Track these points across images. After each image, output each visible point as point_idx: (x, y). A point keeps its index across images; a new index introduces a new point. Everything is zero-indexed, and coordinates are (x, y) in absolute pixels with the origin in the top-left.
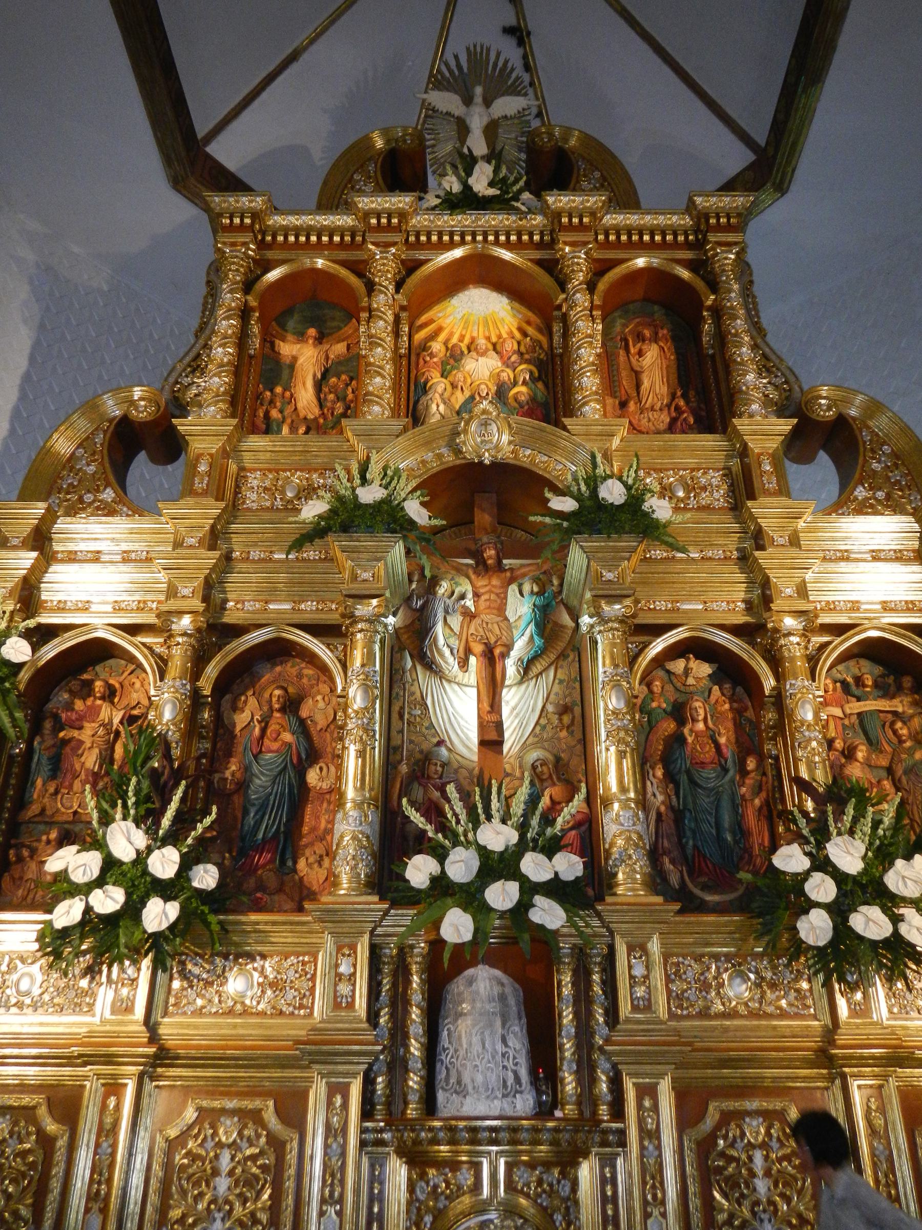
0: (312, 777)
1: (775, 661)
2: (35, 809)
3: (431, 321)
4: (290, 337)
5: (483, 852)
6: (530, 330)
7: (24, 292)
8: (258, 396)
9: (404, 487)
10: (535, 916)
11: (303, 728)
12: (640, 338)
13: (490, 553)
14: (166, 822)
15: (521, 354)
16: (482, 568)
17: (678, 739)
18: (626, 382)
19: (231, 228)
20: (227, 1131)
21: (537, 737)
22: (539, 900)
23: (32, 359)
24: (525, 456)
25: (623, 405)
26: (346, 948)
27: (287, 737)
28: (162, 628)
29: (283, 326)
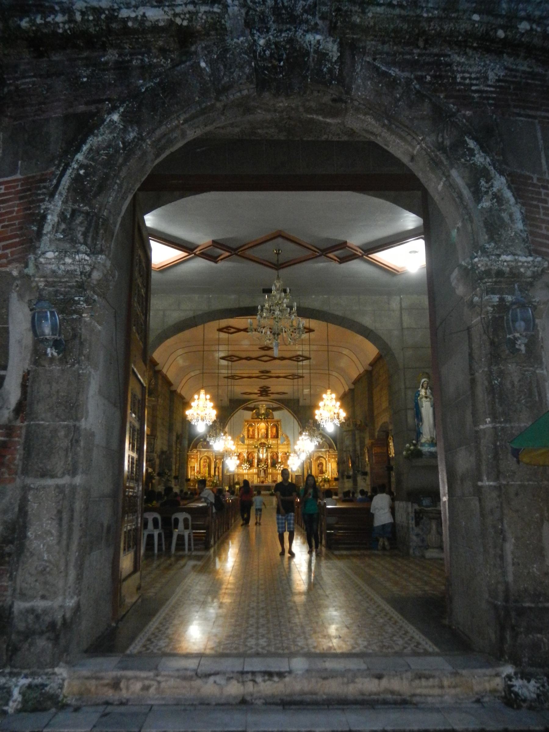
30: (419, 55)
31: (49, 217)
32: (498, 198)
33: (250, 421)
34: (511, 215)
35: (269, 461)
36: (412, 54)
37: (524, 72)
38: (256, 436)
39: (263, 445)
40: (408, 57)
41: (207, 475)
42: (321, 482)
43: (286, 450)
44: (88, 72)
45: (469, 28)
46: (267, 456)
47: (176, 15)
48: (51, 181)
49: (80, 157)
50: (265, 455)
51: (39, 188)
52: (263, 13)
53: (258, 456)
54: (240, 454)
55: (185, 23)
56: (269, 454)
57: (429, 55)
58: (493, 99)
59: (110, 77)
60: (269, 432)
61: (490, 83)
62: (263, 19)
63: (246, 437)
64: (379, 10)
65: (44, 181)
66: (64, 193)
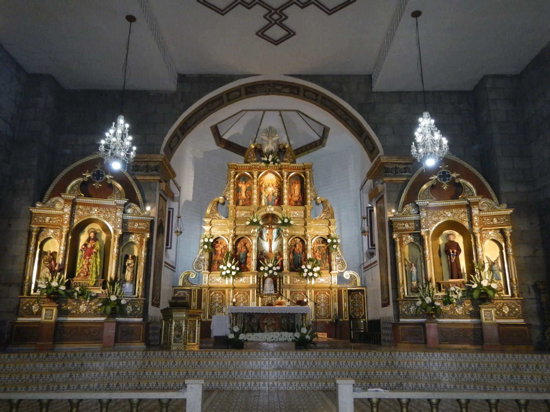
0: (248, 254)
1: (307, 240)
2: (213, 259)
3: (262, 180)
4: (240, 183)
5: (269, 267)
6: (278, 182)
7: (191, 164)
8: (237, 194)
9: (260, 218)
10: (274, 274)
11: (246, 248)
12: (295, 183)
13: (270, 226)
14: (233, 262)
15: (276, 186)
16: (269, 228)
17: (294, 250)
18: (293, 192)
19: (231, 168)
20: (241, 295)
21: (276, 249)
22: (275, 272)
23: (194, 177)
24: (276, 213)
25: (292, 196)
26: (254, 276)
27: (245, 250)
28: (228, 235)
29: (239, 180)
33: (243, 168)
35: (285, 256)
38: (255, 202)
39: (270, 219)
41: (92, 279)
42: (460, 302)
43: (324, 232)
46: (281, 245)
50: (275, 245)
53: (259, 245)
54: (216, 240)
56: (285, 241)
60: (285, 191)
63: (232, 202)
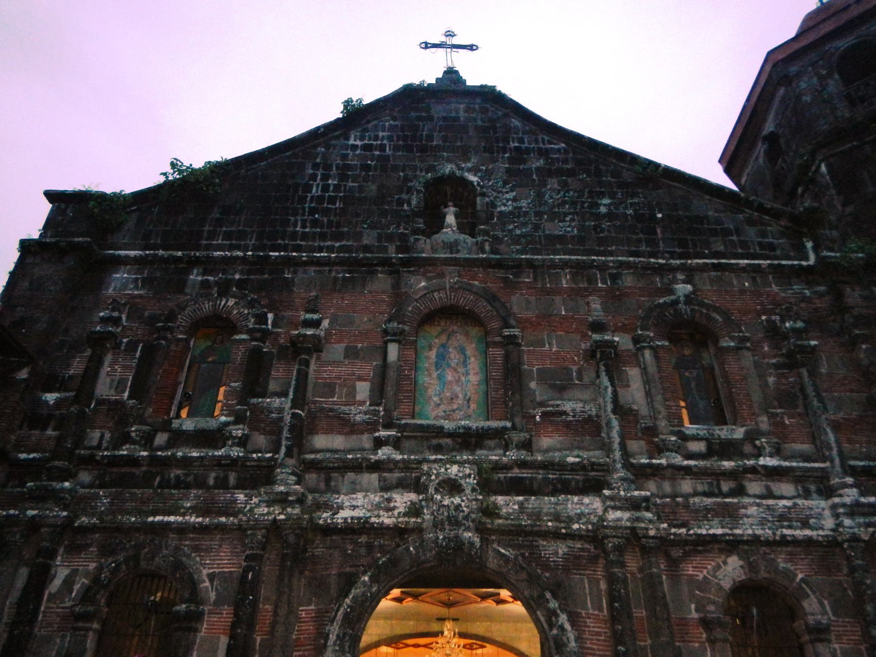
30: (522, 541)
31: (331, 636)
32: (562, 628)
34: (568, 638)
36: (518, 540)
37: (578, 548)
40: (516, 542)
44: (352, 547)
45: (547, 529)
47: (398, 522)
48: (332, 613)
49: (348, 601)
51: (325, 617)
52: (442, 519)
55: (403, 526)
57: (527, 541)
58: (562, 565)
59: (363, 551)
61: (560, 556)
62: (442, 523)
64: (500, 521)
65: (327, 612)
66: (340, 622)
